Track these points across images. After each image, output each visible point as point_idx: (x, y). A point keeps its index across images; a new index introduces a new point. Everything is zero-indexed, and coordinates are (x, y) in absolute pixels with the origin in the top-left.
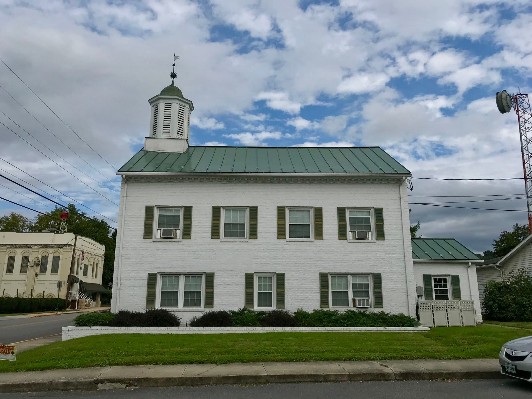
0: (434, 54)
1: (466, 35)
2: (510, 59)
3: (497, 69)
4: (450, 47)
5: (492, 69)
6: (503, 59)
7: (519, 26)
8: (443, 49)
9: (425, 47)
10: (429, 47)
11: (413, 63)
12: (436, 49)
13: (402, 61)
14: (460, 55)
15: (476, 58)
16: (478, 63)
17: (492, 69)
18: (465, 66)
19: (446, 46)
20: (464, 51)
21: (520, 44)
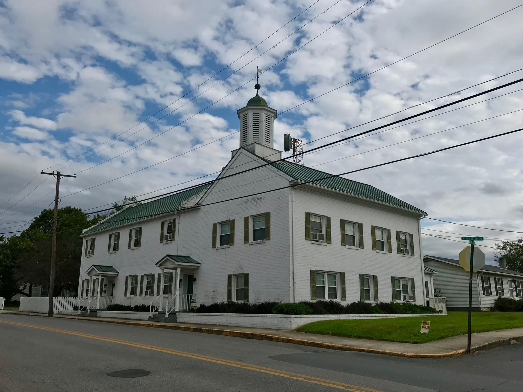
0: (85, 66)
1: (116, 61)
2: (151, 93)
3: (143, 99)
4: (100, 66)
5: (137, 97)
6: (146, 92)
7: (160, 69)
8: (94, 66)
9: (78, 58)
10: (80, 59)
11: (65, 67)
12: (89, 62)
13: (54, 61)
14: (110, 76)
15: (123, 83)
16: (125, 87)
17: (137, 97)
18: (113, 87)
19: (97, 63)
20: (115, 73)
21: (159, 83)
